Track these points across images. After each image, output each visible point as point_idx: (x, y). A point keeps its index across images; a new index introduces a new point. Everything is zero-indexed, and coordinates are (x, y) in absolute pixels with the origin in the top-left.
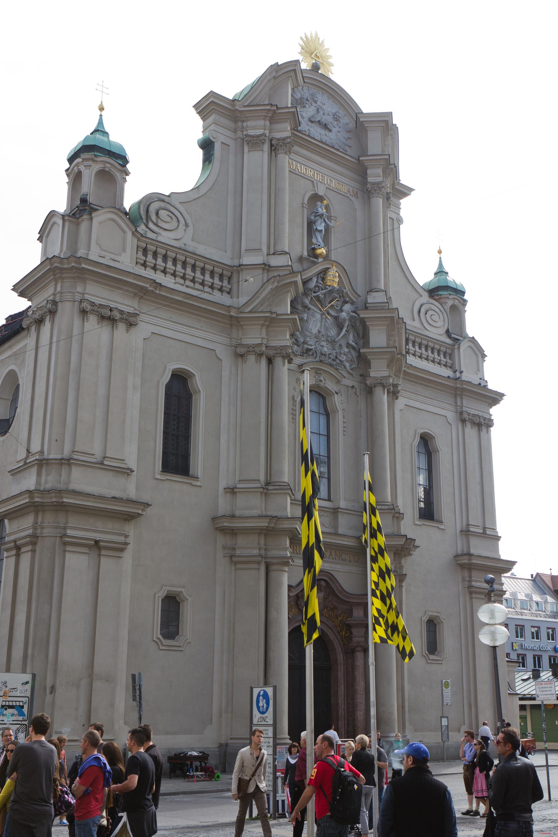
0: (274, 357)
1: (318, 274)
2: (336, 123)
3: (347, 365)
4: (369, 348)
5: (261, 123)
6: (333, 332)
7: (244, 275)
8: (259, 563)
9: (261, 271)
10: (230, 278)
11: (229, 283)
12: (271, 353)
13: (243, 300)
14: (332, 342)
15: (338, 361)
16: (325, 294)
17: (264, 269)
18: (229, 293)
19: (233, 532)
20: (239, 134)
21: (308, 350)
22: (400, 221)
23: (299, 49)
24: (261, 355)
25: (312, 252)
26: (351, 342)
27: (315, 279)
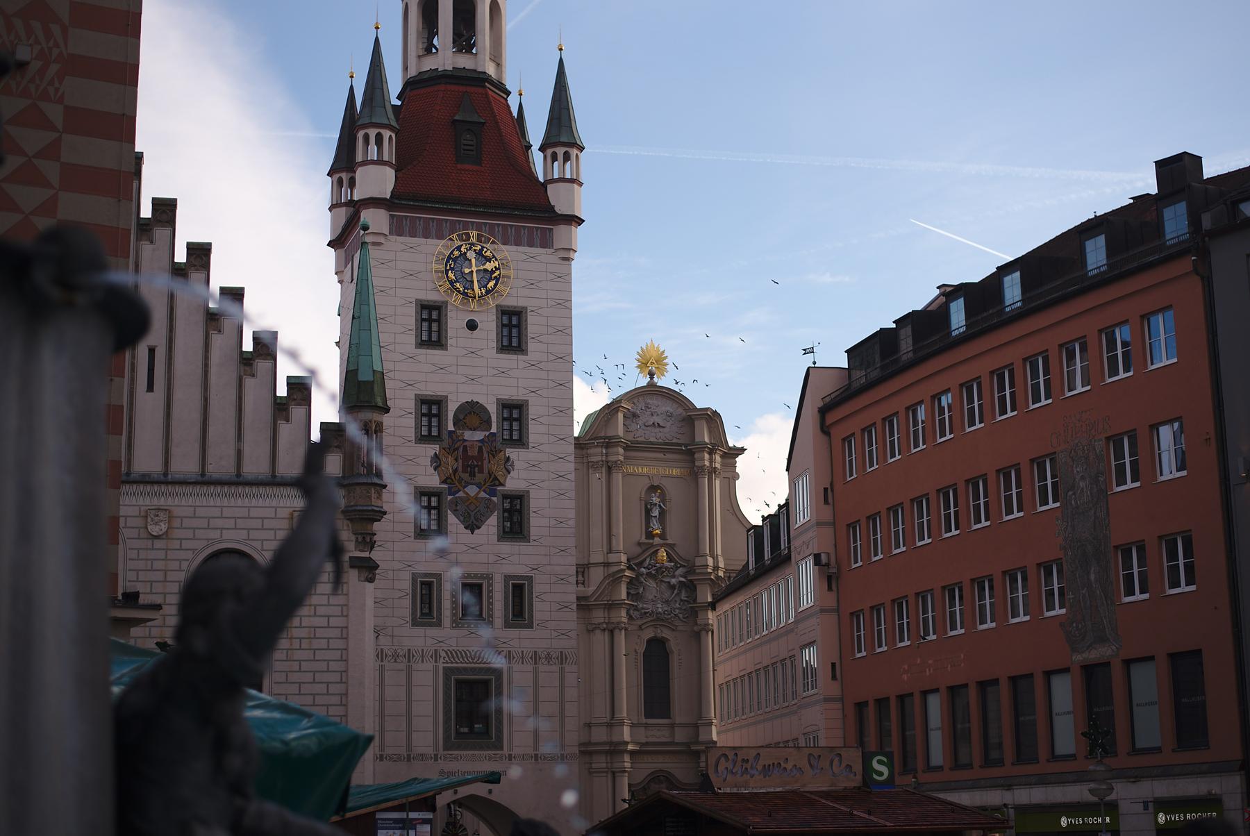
0: (614, 628)
1: (651, 555)
2: (669, 418)
3: (681, 616)
4: (697, 603)
5: (599, 450)
6: (667, 594)
7: (592, 570)
8: (607, 772)
9: (602, 568)
10: (583, 572)
11: (583, 576)
12: (611, 627)
13: (592, 589)
14: (667, 602)
15: (672, 615)
16: (656, 570)
17: (604, 566)
18: (583, 584)
19: (590, 753)
20: (585, 460)
21: (646, 613)
22: (736, 476)
23: (636, 363)
24: (604, 630)
25: (650, 535)
26: (682, 598)
27: (648, 560)
